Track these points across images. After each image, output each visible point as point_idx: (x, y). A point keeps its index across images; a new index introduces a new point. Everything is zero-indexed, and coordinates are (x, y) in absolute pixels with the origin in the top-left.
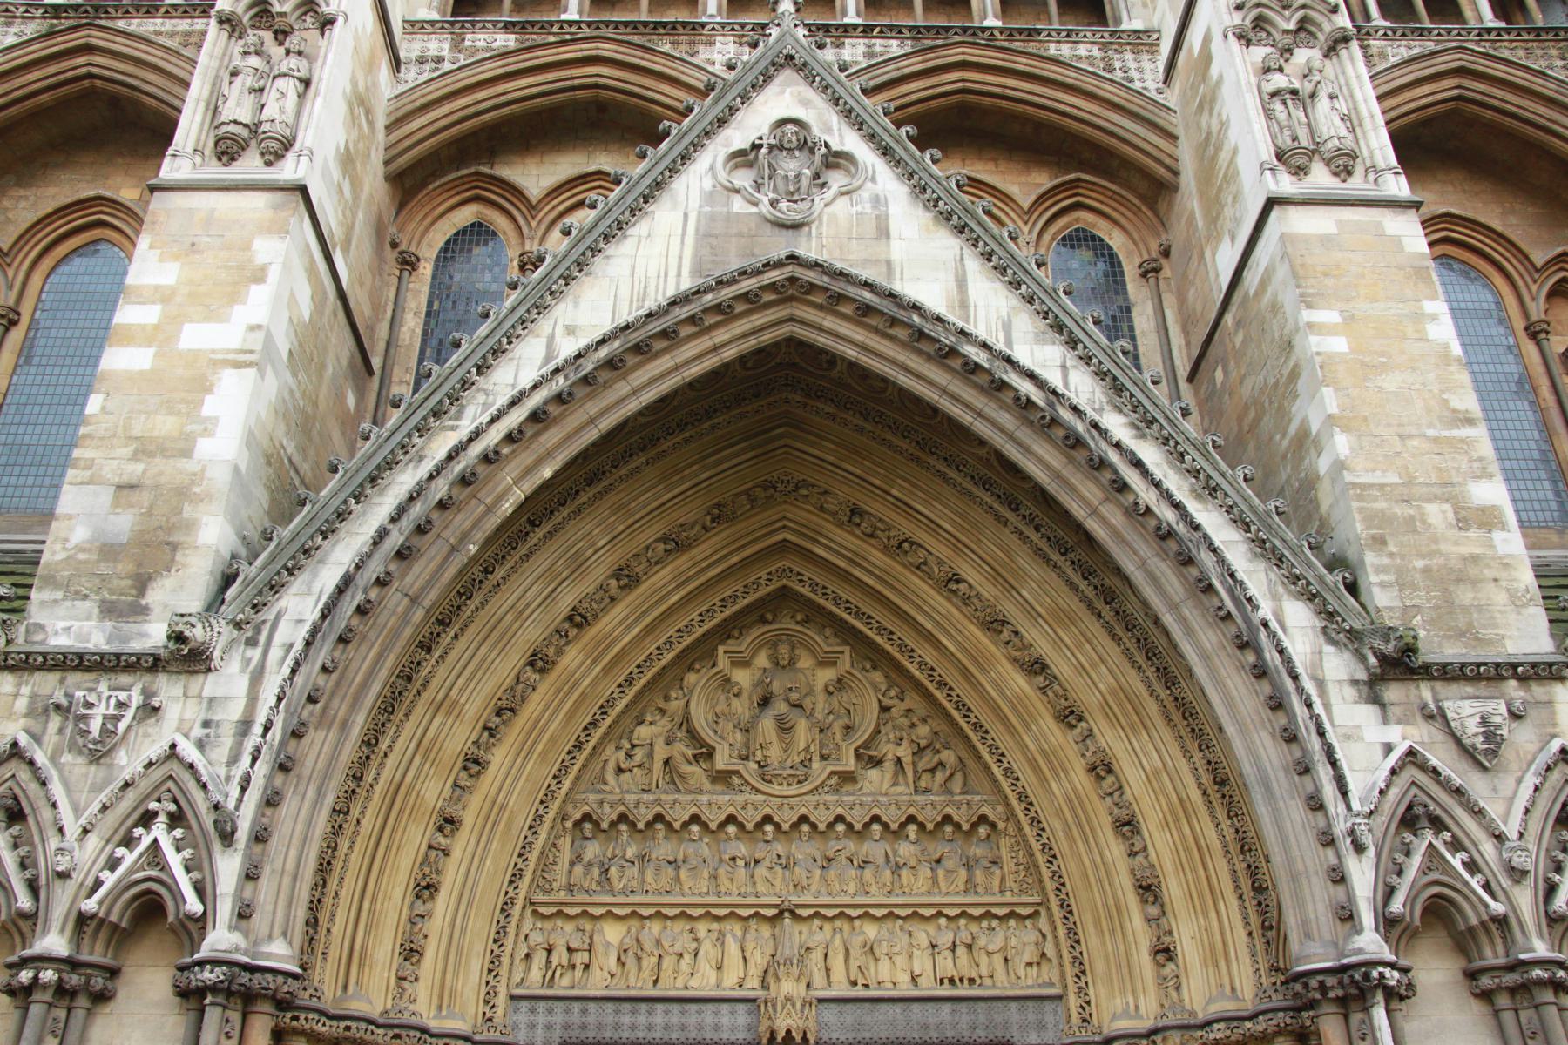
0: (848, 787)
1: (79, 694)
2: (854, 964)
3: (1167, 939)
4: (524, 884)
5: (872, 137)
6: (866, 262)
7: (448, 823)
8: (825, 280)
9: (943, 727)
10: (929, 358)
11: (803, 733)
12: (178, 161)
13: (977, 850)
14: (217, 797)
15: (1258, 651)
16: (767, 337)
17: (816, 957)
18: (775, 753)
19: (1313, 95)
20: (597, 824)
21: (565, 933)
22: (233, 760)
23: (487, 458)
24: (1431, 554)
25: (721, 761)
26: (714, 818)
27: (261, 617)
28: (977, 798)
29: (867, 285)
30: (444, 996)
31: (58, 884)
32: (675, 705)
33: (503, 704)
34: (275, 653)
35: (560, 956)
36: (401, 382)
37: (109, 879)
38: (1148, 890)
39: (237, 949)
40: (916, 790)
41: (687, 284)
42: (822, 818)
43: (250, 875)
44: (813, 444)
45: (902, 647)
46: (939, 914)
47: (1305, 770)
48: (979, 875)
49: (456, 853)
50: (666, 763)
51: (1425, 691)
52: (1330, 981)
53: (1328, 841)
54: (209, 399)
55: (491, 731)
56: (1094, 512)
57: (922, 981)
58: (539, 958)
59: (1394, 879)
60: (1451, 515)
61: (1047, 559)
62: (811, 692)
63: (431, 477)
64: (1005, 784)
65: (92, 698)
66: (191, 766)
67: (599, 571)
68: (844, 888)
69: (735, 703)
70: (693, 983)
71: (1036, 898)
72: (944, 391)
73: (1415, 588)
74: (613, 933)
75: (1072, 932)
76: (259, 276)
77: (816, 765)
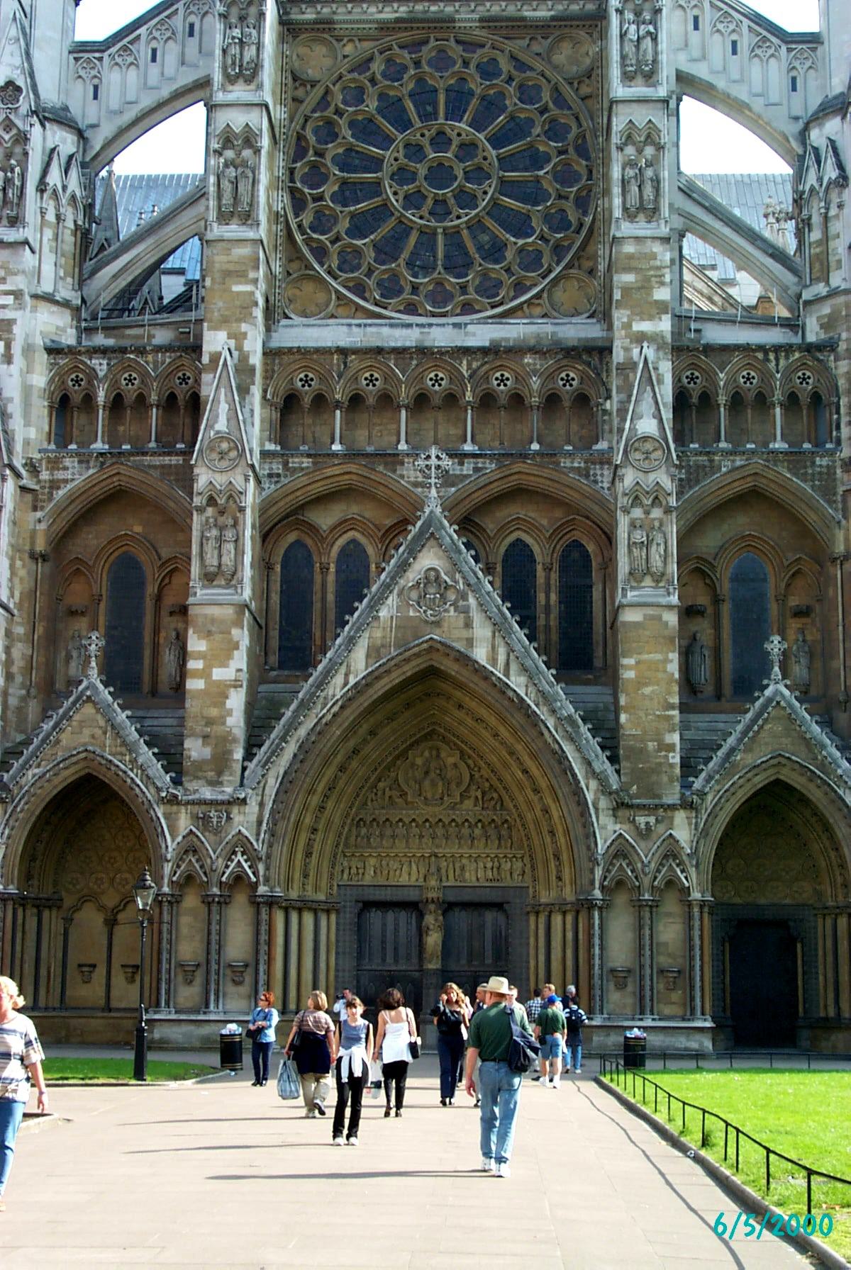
6: (459, 639)
7: (314, 830)
17: (443, 871)
20: (365, 822)
22: (258, 834)
23: (326, 724)
26: (407, 820)
28: (505, 812)
30: (317, 888)
32: (393, 775)
34: (266, 798)
35: (354, 871)
37: (228, 872)
38: (557, 857)
43: (267, 868)
49: (318, 840)
50: (390, 797)
54: (228, 701)
58: (347, 872)
74: (372, 861)
75: (532, 866)
76: (237, 648)
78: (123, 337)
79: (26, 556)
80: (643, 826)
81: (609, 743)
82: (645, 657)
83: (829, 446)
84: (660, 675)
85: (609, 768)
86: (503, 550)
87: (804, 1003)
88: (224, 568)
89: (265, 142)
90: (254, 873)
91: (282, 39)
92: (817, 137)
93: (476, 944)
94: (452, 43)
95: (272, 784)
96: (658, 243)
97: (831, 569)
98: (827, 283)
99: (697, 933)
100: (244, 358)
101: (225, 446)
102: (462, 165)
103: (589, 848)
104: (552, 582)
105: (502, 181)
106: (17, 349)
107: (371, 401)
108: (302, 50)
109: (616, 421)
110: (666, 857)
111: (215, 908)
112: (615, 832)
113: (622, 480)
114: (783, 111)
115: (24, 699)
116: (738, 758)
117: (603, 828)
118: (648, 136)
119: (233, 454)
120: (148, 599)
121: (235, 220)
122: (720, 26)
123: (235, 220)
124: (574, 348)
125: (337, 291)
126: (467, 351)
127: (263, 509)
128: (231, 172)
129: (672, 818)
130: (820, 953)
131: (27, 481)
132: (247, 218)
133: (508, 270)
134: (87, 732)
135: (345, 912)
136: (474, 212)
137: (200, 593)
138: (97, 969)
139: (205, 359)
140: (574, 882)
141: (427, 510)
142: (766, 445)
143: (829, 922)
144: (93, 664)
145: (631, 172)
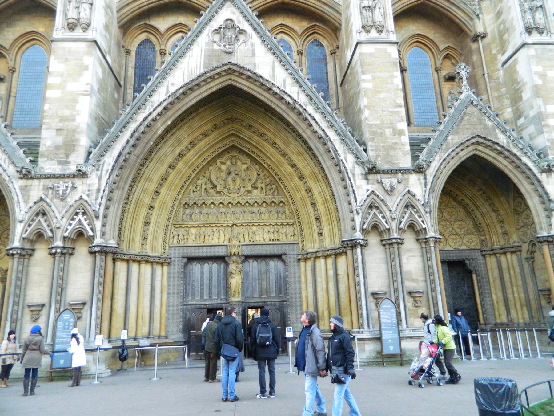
0: (249, 194)
1: (56, 184)
2: (250, 236)
3: (321, 231)
4: (171, 221)
5: (251, 25)
6: (249, 63)
7: (151, 208)
8: (238, 69)
9: (273, 179)
10: (265, 90)
11: (238, 181)
12: (58, 32)
13: (280, 209)
14: (93, 208)
15: (340, 167)
16: (224, 84)
17: (241, 235)
18: (231, 186)
19: (375, 7)
20: (188, 205)
21: (182, 231)
22: (97, 199)
23: (154, 120)
24: (385, 142)
26: (217, 203)
27: (99, 163)
29: (249, 70)
30: (153, 248)
31: (58, 230)
32: (207, 175)
33: (163, 178)
34: (104, 172)
35: (181, 237)
36: (130, 89)
37: (70, 228)
38: (318, 219)
39: (102, 243)
40: (266, 195)
41: (202, 71)
43: (104, 225)
44: (238, 109)
45: (262, 160)
46: (271, 224)
48: (280, 216)
49: (154, 214)
51: (378, 177)
52: (349, 243)
53: (352, 212)
54: (77, 105)
56: (304, 131)
57: (266, 240)
58: (176, 238)
59: (365, 220)
60: (392, 132)
61: (296, 140)
62: (241, 171)
63: (139, 126)
64: (286, 194)
65: (59, 186)
66: (86, 201)
67: (186, 143)
68: (248, 219)
69: (222, 174)
70: (213, 242)
71: (293, 221)
72: (269, 99)
73: (380, 151)
74: (193, 231)
75: (301, 229)
76: (86, 68)
77: (242, 189)
80: (388, 186)
85: (361, 148)
87: (483, 313)
88: (81, 20)
90: (92, 229)
93: (264, 283)
95: (109, 160)
104: (303, 62)
110: (407, 207)
112: (368, 190)
116: (450, 138)
135: (174, 265)
140: (332, 235)
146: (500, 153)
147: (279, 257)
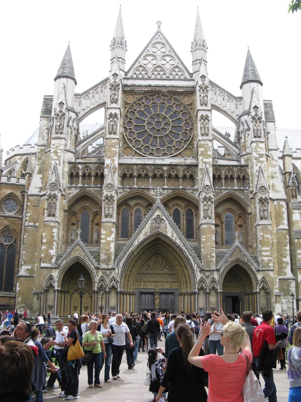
7: (130, 276)
11: (159, 265)
13: (173, 276)
17: (159, 285)
21: (139, 283)
22: (118, 276)
25: (152, 268)
30: (130, 289)
32: (147, 263)
35: (138, 285)
37: (111, 285)
38: (186, 282)
41: (149, 234)
42: (160, 273)
43: (120, 285)
47: (194, 278)
50: (147, 268)
55: (132, 268)
74: (143, 283)
76: (113, 233)
78: (85, 160)
79: (63, 211)
81: (199, 256)
82: (207, 236)
83: (247, 188)
84: (211, 240)
85: (200, 262)
86: (173, 210)
89: (119, 116)
91: (122, 94)
92: (243, 119)
93: (167, 302)
94: (161, 96)
95: (121, 265)
96: (209, 141)
97: (248, 216)
98: (246, 152)
99: (219, 299)
100: (115, 166)
101: (110, 186)
102: (163, 123)
103: (195, 280)
105: (172, 126)
106: (61, 162)
107: (143, 176)
108: (127, 96)
109: (200, 182)
110: (212, 282)
111: (107, 294)
113: (202, 195)
114: (235, 114)
115: (62, 244)
117: (198, 275)
118: (206, 118)
119: (112, 188)
120: (90, 221)
121: (112, 134)
122: (220, 94)
123: (112, 134)
124: (190, 165)
125: (135, 150)
126: (165, 165)
127: (118, 201)
128: (112, 123)
129: (213, 273)
130: (245, 303)
131: (63, 193)
132: (115, 133)
133: (174, 146)
134: (77, 252)
136: (166, 133)
137: (104, 219)
138: (78, 308)
139: (105, 165)
140: (190, 288)
141: (157, 201)
142: (233, 187)
143: (247, 297)
144: (79, 236)
145: (203, 126)
146: (245, 264)
147: (172, 293)
